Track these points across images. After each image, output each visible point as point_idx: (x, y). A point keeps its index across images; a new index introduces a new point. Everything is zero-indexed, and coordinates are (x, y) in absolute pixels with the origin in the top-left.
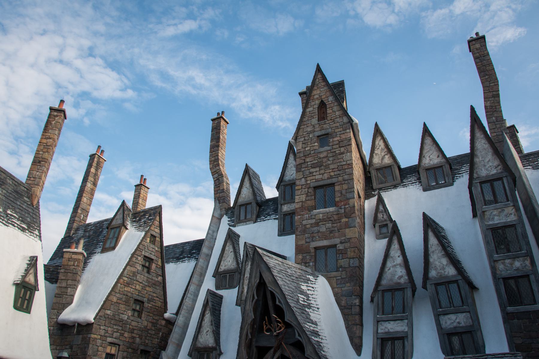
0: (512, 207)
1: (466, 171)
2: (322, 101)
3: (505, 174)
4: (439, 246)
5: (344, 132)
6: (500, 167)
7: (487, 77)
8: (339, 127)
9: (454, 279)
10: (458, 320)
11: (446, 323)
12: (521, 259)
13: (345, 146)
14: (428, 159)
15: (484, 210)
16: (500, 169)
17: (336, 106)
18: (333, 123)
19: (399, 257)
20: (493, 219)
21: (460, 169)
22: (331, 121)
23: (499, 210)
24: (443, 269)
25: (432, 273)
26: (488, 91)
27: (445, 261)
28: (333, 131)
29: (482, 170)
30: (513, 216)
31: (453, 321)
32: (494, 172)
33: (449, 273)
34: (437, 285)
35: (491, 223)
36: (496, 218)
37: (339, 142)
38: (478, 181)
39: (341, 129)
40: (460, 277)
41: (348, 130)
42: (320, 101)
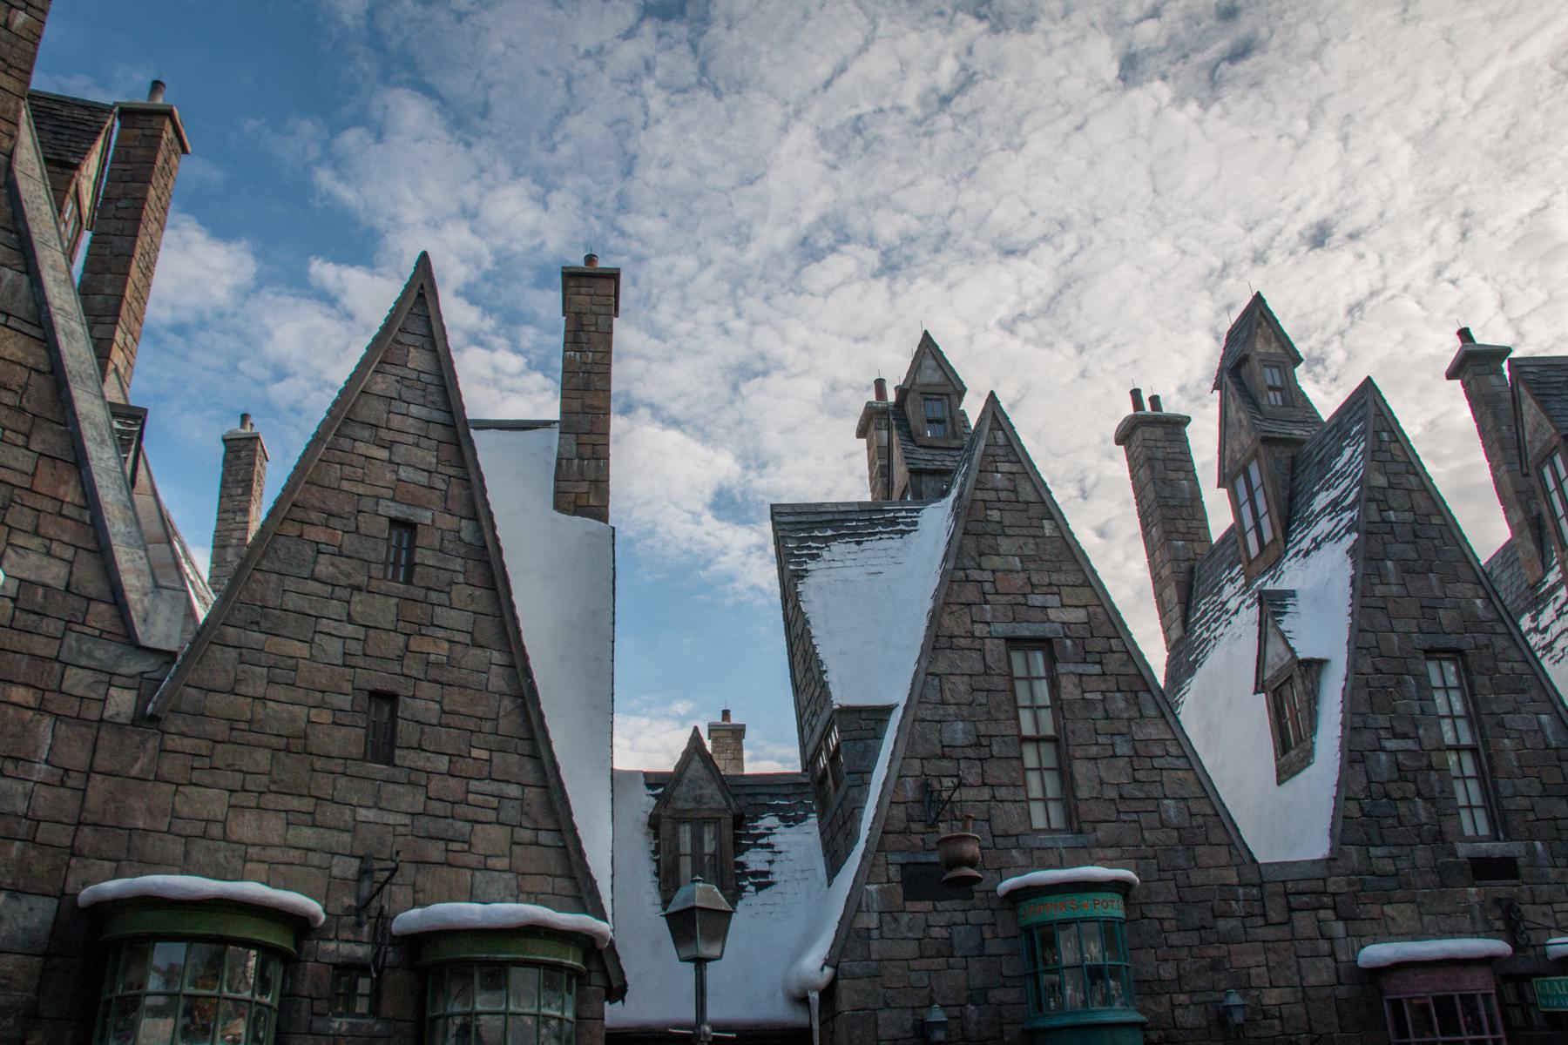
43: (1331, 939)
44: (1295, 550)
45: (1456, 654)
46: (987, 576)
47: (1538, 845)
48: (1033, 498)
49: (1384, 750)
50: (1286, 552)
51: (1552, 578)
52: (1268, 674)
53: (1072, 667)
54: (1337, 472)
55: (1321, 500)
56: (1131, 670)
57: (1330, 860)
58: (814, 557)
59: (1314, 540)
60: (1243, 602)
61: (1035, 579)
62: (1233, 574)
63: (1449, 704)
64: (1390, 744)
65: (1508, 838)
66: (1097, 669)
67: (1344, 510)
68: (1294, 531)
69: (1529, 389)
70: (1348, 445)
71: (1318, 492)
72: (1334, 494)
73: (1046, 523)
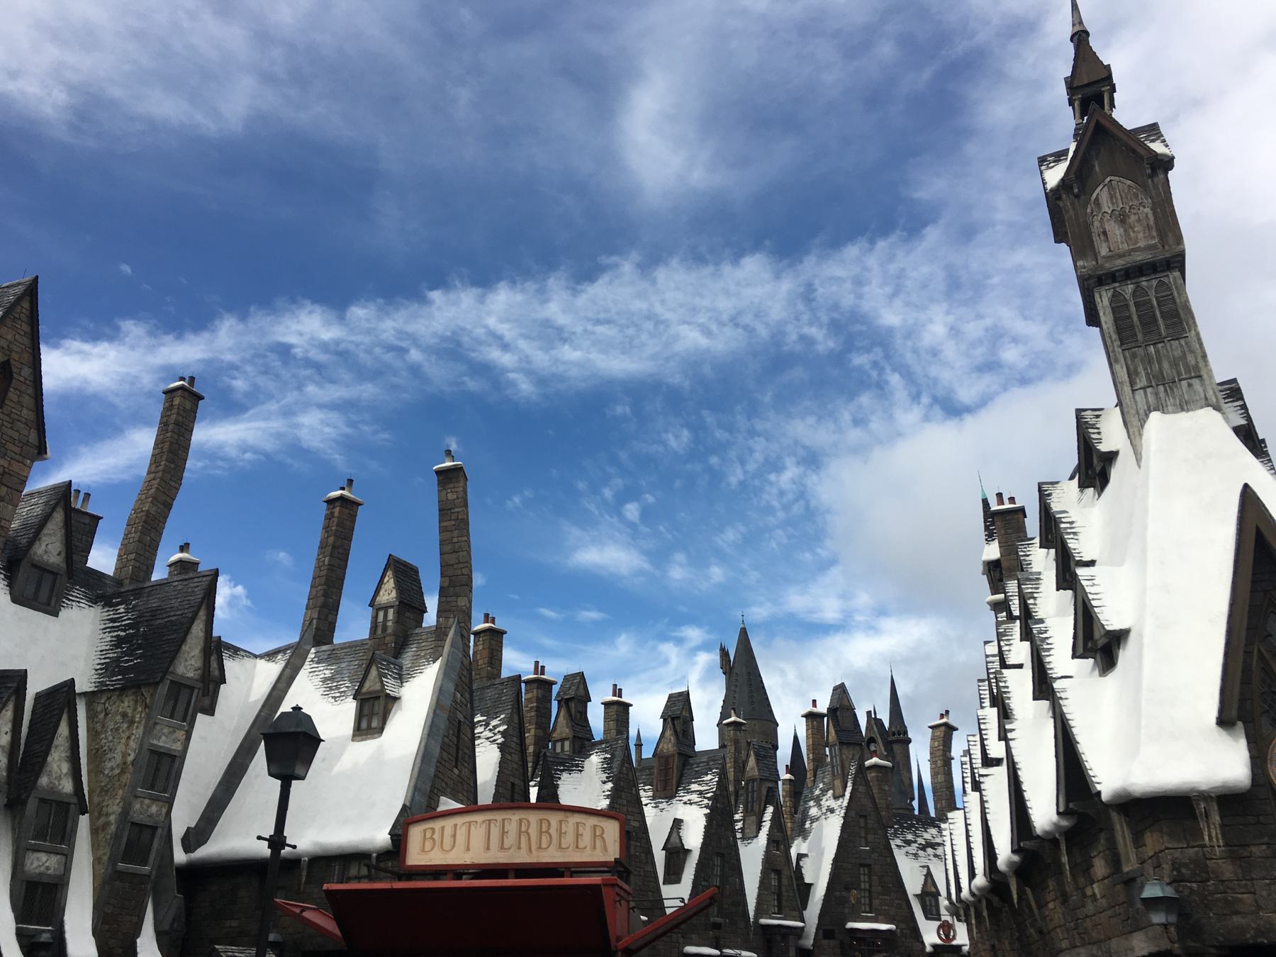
0: (184, 733)
1: (78, 600)
2: (8, 360)
3: (199, 685)
4: (68, 742)
5: (20, 458)
6: (199, 671)
7: (172, 466)
8: (17, 442)
9: (66, 800)
10: (47, 864)
11: (32, 864)
12: (160, 803)
13: (11, 488)
14: (43, 547)
15: (157, 721)
16: (198, 675)
17: (28, 395)
18: (9, 426)
19: (6, 734)
20: (160, 737)
21: (70, 591)
22: (7, 418)
23: (171, 729)
24: (59, 778)
25: (43, 779)
26: (163, 490)
27: (65, 767)
28: (4, 442)
29: (180, 664)
30: (179, 743)
31: (41, 864)
32: (191, 674)
33: (63, 788)
34: (42, 800)
35: (155, 742)
36: (164, 738)
37: (4, 472)
38: (170, 678)
39: (17, 450)
40: (75, 800)
41: (29, 461)
42: (6, 358)
43: (679, 943)
44: (680, 798)
45: (722, 856)
46: (618, 806)
47: (727, 920)
49: (701, 885)
50: (676, 797)
51: (737, 817)
52: (669, 846)
53: (634, 842)
54: (703, 781)
55: (694, 787)
56: (647, 846)
58: (560, 778)
59: (689, 800)
60: (650, 803)
62: (646, 788)
63: (718, 871)
64: (703, 883)
65: (721, 917)
66: (639, 844)
67: (705, 798)
68: (681, 790)
69: (754, 752)
71: (694, 783)
73: (634, 788)
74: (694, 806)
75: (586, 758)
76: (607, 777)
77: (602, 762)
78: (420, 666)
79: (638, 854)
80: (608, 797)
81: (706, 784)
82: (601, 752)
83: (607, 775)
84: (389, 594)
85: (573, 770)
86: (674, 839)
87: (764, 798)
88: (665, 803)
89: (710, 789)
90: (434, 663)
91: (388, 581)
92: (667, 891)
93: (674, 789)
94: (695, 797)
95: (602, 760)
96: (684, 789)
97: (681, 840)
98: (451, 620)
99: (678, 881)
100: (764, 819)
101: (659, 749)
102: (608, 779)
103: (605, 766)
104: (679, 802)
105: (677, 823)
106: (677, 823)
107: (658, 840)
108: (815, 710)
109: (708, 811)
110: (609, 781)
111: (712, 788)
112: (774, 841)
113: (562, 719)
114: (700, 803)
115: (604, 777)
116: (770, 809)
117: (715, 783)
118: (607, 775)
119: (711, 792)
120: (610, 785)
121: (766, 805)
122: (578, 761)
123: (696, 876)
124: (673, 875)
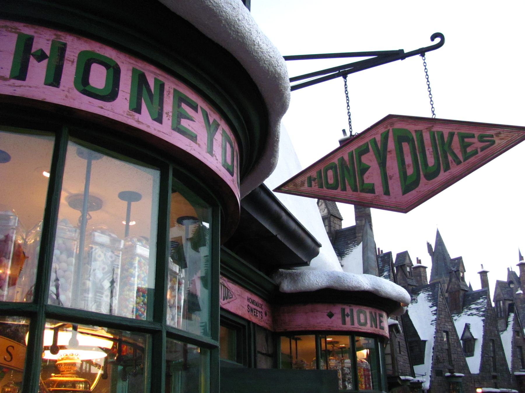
44: (465, 313)
47: (499, 374)
48: (445, 304)
50: (462, 312)
52: (464, 338)
54: (478, 303)
55: (473, 306)
57: (478, 374)
59: (471, 313)
61: (446, 320)
64: (486, 355)
66: (452, 337)
68: (465, 309)
70: (482, 299)
72: (477, 306)
73: (447, 309)
74: (474, 316)
75: (418, 296)
76: (432, 304)
77: (428, 297)
78: (350, 248)
79: (453, 342)
80: (435, 314)
81: (480, 304)
82: (425, 291)
83: (431, 303)
84: (323, 212)
85: (413, 302)
86: (467, 334)
87: (507, 310)
88: (456, 316)
89: (483, 306)
90: (358, 245)
91: (321, 205)
92: (469, 360)
93: (461, 309)
94: (474, 312)
95: (427, 296)
96: (466, 308)
97: (471, 334)
98: (363, 222)
99: (472, 355)
100: (509, 320)
101: (449, 289)
102: (433, 305)
103: (430, 298)
104: (464, 315)
105: (467, 327)
106: (467, 327)
107: (460, 334)
108: (522, 261)
109: (483, 318)
110: (434, 306)
111: (484, 306)
112: (516, 331)
113: (400, 276)
114: (478, 314)
115: (430, 304)
116: (512, 315)
117: (485, 303)
118: (431, 303)
119: (485, 308)
120: (435, 308)
121: (509, 313)
122: (414, 297)
123: (483, 352)
124: (469, 351)
